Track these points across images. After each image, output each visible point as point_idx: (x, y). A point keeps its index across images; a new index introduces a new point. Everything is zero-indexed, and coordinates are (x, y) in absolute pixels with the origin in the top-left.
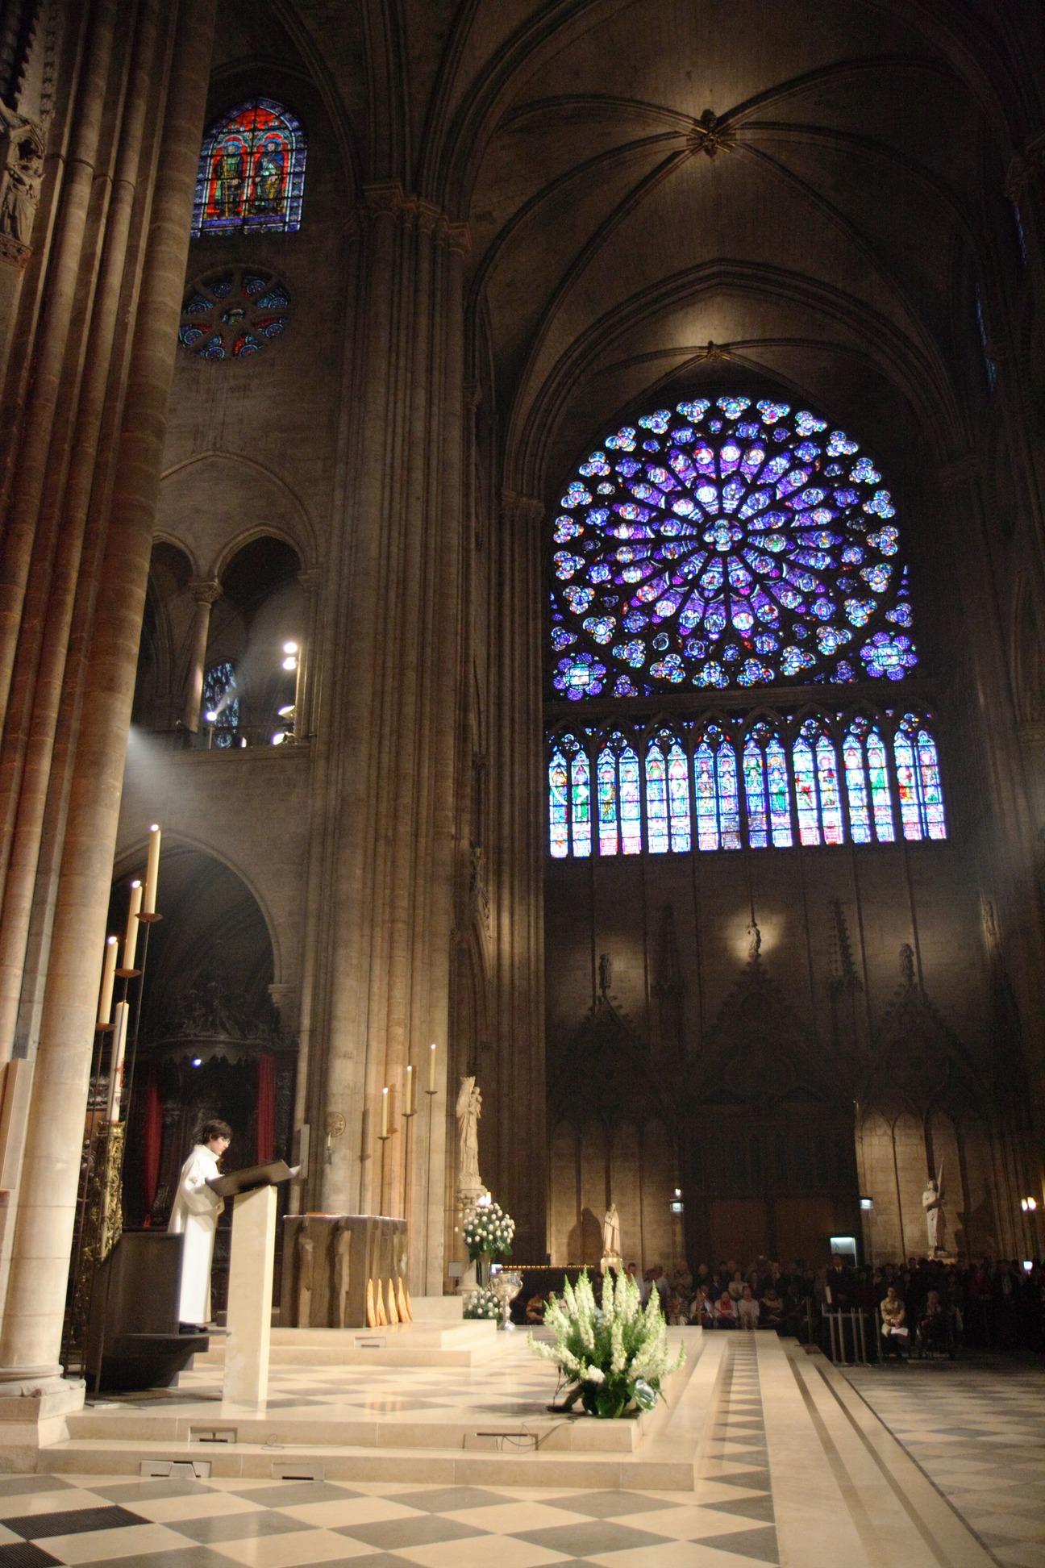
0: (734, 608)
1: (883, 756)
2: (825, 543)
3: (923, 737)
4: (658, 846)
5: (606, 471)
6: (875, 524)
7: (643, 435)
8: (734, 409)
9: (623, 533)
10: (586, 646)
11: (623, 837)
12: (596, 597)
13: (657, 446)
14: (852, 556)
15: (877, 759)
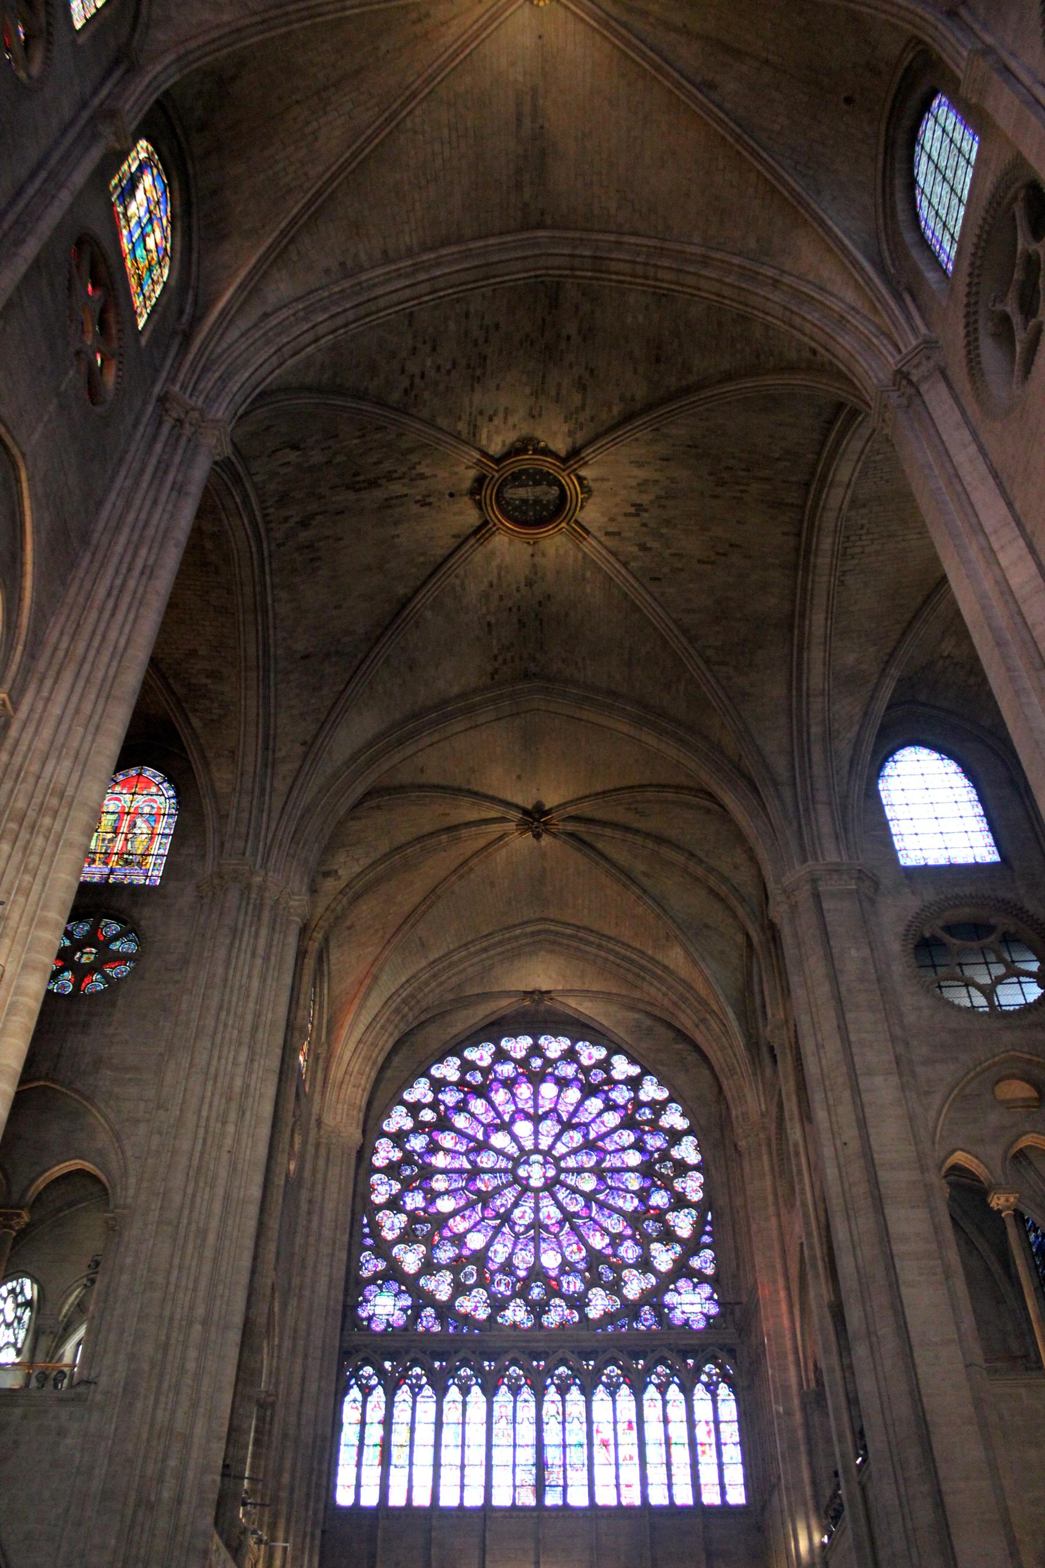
0: (543, 1245)
5: (429, 1098)
6: (682, 1168)
7: (467, 1066)
9: (440, 1160)
13: (479, 1077)
14: (659, 1199)
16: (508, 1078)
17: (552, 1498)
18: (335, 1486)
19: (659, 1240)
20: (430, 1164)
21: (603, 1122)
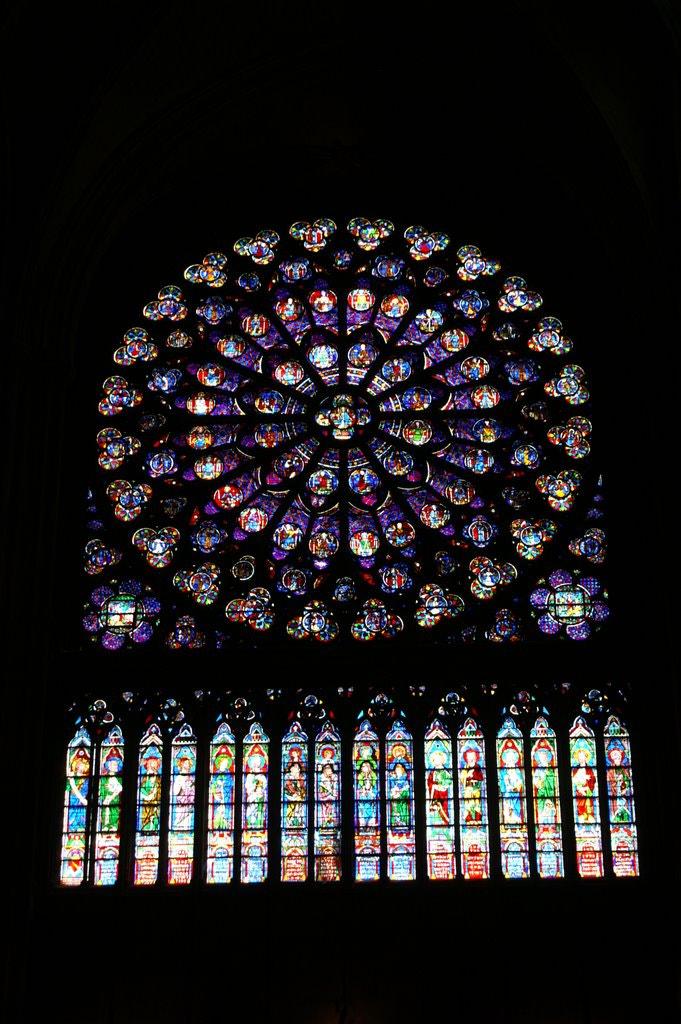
0: (354, 524)
1: (554, 753)
2: (489, 436)
3: (613, 727)
4: (219, 872)
6: (560, 411)
7: (239, 266)
8: (370, 237)
10: (133, 574)
11: (167, 855)
12: (154, 498)
13: (257, 281)
14: (524, 458)
15: (542, 757)
17: (366, 872)
18: (56, 863)
19: (522, 516)
21: (443, 346)
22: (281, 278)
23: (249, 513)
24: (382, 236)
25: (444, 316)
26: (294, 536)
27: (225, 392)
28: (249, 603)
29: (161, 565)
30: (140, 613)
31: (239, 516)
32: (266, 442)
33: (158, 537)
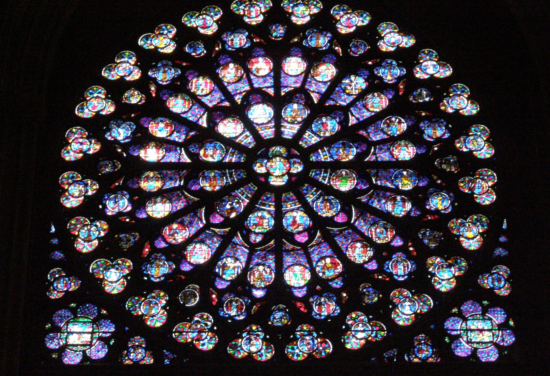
0: (288, 260)
2: (407, 185)
5: (136, 75)
6: (470, 165)
7: (186, 36)
9: (151, 154)
10: (90, 297)
12: (110, 233)
14: (439, 203)
16: (241, 49)
19: (436, 253)
20: (138, 157)
21: (365, 106)
22: (223, 46)
23: (195, 247)
24: (311, 13)
25: (366, 80)
26: (234, 268)
27: (174, 143)
28: (194, 326)
29: (115, 292)
30: (96, 332)
31: (185, 249)
32: (210, 186)
33: (113, 266)
